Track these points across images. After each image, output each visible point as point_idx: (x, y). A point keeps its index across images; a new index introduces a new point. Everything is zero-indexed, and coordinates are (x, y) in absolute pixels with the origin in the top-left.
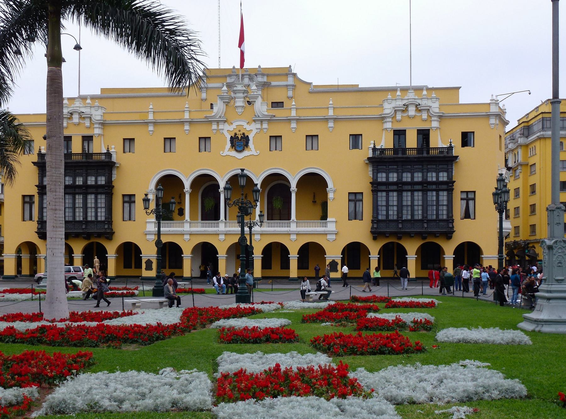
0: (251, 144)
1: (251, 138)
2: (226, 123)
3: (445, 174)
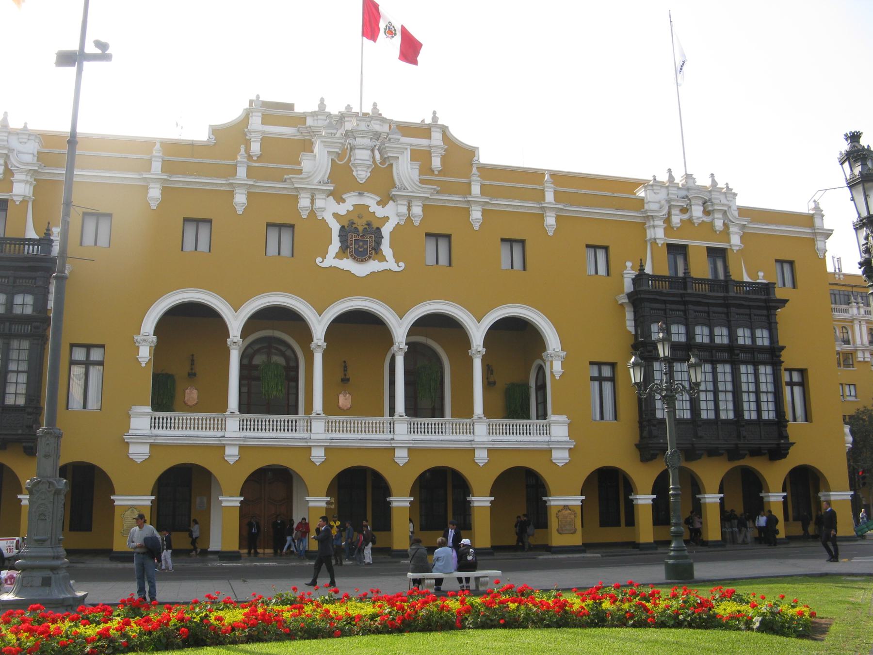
0: (386, 248)
1: (386, 230)
2: (331, 198)
3: (29, 299)
